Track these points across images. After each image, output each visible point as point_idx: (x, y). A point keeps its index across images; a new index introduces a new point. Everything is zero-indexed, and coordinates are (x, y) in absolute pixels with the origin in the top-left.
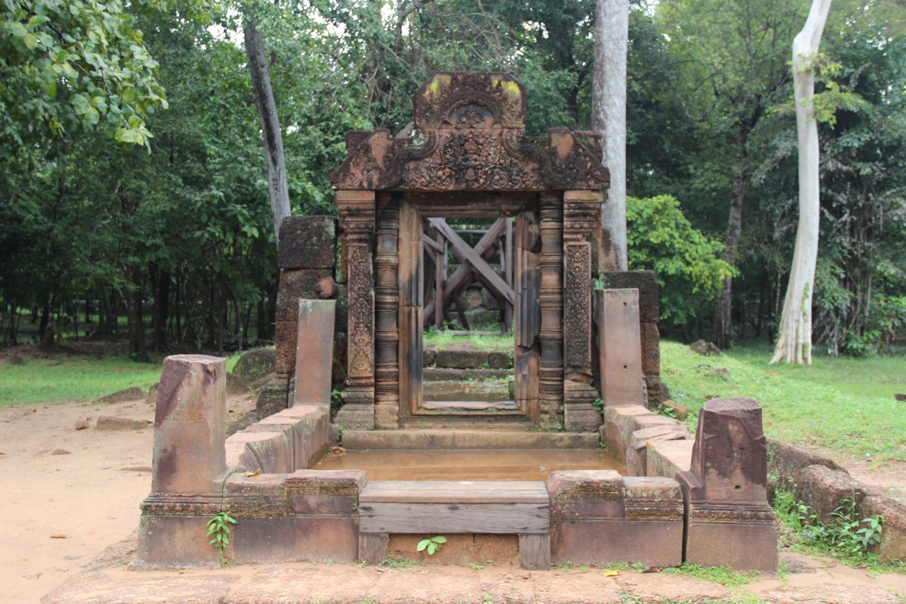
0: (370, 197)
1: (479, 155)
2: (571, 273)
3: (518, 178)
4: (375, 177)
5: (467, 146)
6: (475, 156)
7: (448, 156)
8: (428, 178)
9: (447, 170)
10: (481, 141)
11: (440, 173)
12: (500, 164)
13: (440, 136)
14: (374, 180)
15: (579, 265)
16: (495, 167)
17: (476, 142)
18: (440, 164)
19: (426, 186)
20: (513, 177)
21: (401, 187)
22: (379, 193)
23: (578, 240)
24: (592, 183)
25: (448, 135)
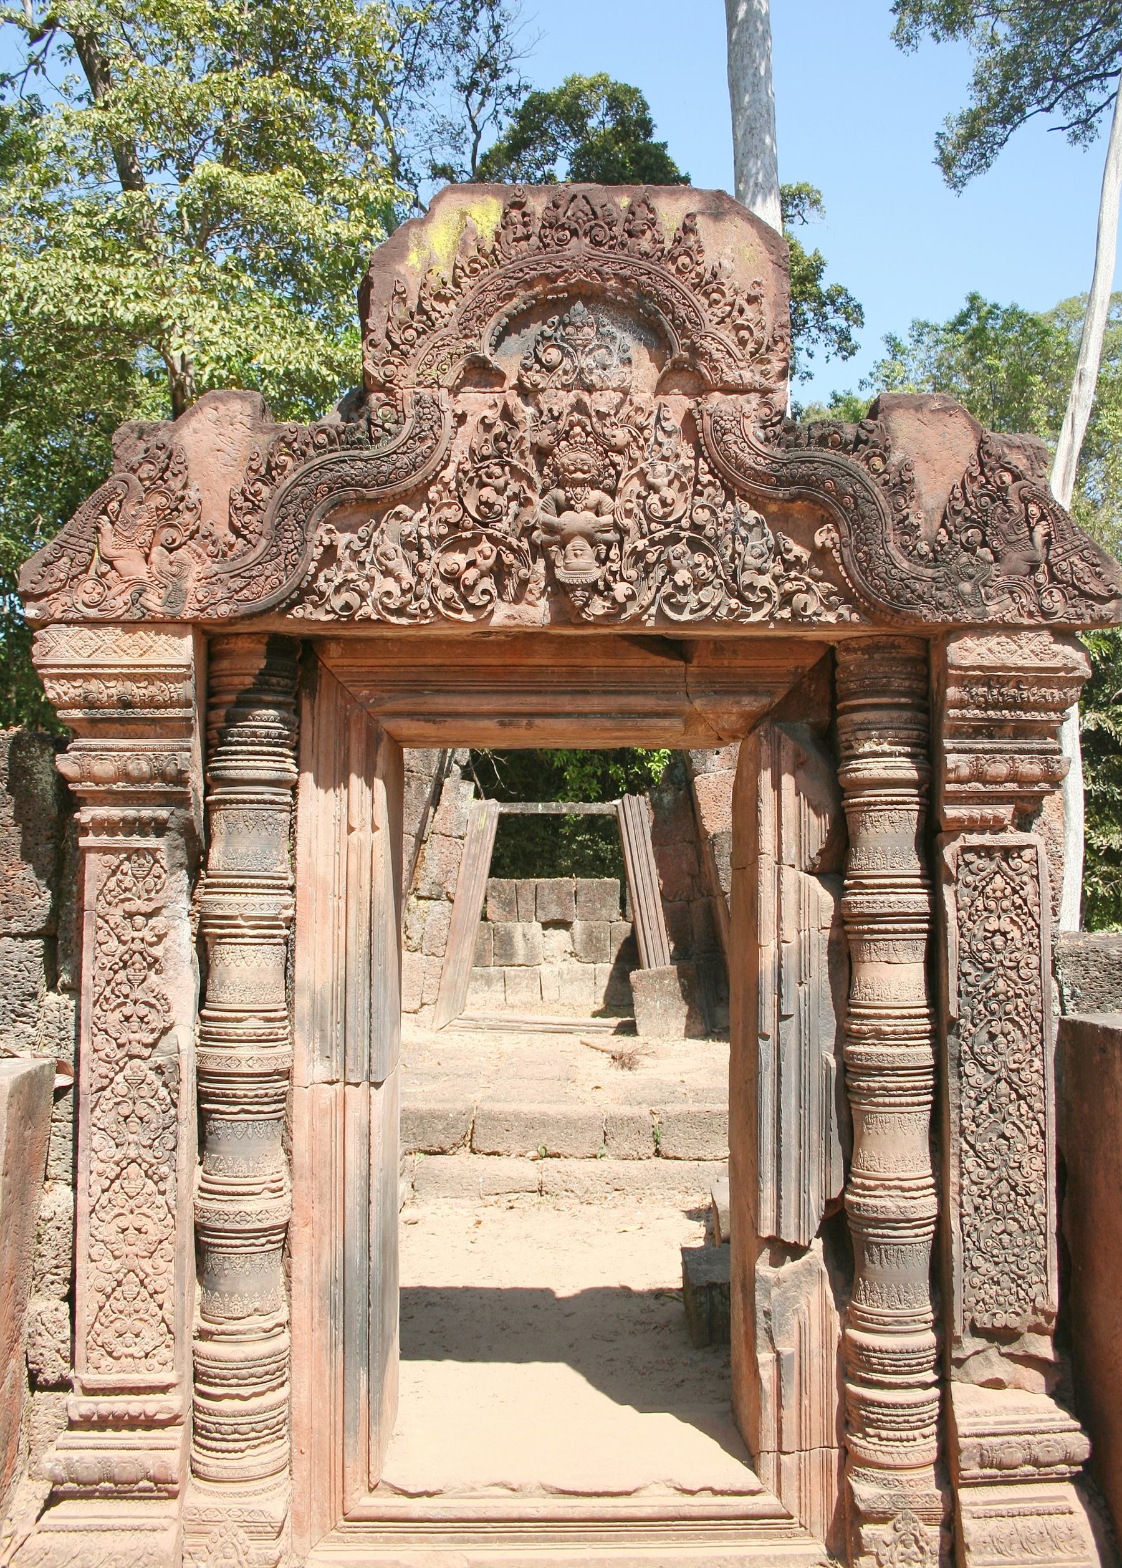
0: (181, 650)
1: (613, 492)
2: (974, 958)
3: (765, 581)
4: (195, 568)
5: (566, 456)
6: (595, 495)
7: (487, 493)
8: (406, 573)
9: (485, 545)
10: (621, 436)
11: (458, 559)
12: (696, 527)
13: (461, 419)
14: (190, 584)
15: (1005, 924)
16: (674, 539)
17: (599, 438)
18: (455, 526)
19: (400, 612)
20: (745, 578)
21: (298, 612)
22: (212, 641)
23: (997, 827)
24: (1055, 601)
25: (492, 415)
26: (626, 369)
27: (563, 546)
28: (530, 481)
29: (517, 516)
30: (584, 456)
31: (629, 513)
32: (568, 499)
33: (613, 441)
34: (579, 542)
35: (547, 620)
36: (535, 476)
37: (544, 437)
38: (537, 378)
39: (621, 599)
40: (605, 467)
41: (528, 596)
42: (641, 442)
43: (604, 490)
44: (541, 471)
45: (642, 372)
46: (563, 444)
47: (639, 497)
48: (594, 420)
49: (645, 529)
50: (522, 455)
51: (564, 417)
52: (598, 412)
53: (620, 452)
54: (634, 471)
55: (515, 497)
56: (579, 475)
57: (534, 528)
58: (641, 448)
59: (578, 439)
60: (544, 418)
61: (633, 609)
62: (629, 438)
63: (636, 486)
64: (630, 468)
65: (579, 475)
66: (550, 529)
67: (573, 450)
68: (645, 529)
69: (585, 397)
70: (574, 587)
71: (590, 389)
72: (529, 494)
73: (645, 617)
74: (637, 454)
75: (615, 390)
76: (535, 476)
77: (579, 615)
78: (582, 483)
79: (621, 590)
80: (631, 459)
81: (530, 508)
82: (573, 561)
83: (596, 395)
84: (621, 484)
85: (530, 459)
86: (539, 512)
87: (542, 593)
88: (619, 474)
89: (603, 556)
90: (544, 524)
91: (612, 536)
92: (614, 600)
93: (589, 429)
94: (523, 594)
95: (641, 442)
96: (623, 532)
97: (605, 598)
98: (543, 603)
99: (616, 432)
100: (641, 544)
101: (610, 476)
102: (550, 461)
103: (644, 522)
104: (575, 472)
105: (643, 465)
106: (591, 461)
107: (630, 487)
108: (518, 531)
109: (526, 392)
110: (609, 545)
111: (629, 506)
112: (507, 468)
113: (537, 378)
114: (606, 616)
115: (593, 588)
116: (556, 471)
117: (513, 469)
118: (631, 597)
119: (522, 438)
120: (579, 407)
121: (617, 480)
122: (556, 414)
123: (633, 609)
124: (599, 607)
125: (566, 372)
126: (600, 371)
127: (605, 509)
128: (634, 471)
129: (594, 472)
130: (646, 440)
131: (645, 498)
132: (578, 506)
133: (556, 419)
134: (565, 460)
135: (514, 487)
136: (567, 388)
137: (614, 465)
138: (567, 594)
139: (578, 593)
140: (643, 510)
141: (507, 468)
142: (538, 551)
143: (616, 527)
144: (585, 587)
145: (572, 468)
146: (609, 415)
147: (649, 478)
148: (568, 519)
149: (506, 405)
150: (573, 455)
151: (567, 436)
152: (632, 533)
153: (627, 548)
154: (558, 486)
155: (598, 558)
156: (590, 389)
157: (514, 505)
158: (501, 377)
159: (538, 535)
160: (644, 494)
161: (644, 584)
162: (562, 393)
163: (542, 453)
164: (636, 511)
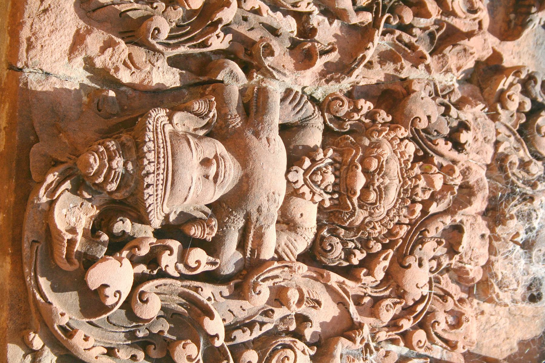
1: (312, 256)
10: (417, 280)
26: (521, 290)
27: (216, 131)
28: (343, 68)
29: (274, 32)
30: (393, 194)
31: (279, 297)
32: (310, 152)
33: (411, 261)
34: (232, 172)
35: (34, 81)
36: (346, 84)
37: (425, 109)
38: (513, 106)
39: (95, 278)
40: (365, 244)
41: (95, 40)
42: (407, 324)
43: (318, 240)
44: (367, 92)
45: (504, 323)
46: (411, 148)
47: (302, 319)
48: (448, 220)
49: (242, 337)
50: (385, 57)
51: (454, 155)
52: (458, 229)
53: (390, 277)
54: (353, 309)
55: (307, 32)
56: (361, 181)
57: (247, 69)
58: (394, 324)
59: (422, 183)
60: (454, 112)
61: (64, 307)
62: (414, 294)
63: (327, 313)
64: (358, 300)
65: (361, 181)
66: (254, 106)
67: (404, 173)
68: (242, 337)
69: (479, 204)
70: (135, 151)
71: (494, 215)
72: (320, 63)
73: (37, 342)
74: (387, 316)
75: (488, 266)
76: (346, 84)
77: (55, 164)
78: (343, 188)
79: (115, 276)
80: (377, 301)
81: (289, 62)
82: (191, 159)
83: (482, 226)
84: (335, 278)
85: (377, 75)
86: (287, 80)
87: (104, 77)
88: (349, 272)
89: (195, 231)
90: (263, 94)
91: (230, 257)
92: (89, 261)
93: (434, 209)
94: (101, 23)
95: (407, 324)
96: (239, 285)
97: (92, 233)
98: (72, 76)
99: (427, 265)
100: (215, 326)
101: (349, 254)
102: (383, 116)
103: (257, 333)
104: (366, 172)
105: (366, 331)
106: (381, 212)
107: (325, 298)
108: (243, 29)
109: (485, 76)
110: (213, 248)
111: (293, 296)
112: (368, 17)
113: (513, 106)
114: (49, 234)
115: (128, 203)
116: (359, 130)
117: (362, 35)
118: (93, 303)
119: (418, 60)
120: (467, 192)
121: (338, 270)
122: (464, 137)
123: (64, 307)
124: (72, 215)
125: (524, 165)
126: (523, 236)
127: (285, 237)
128: (353, 309)
129: (360, 216)
130: (406, 336)
131: (298, 335)
132: (298, 176)
133: (453, 139)
134: (387, 150)
135: (327, 32)
136: (499, 163)
137: (368, 263)
138: (107, 134)
139: (118, 163)
140: (274, 334)
141: (368, 17)
142: (201, 75)
143: (251, 266)
144: (134, 183)
145: (374, 164)
146: (452, 251)
147: (342, 346)
148: (272, 154)
149: (470, 35)
150: (394, 168)
151: (423, 158)
152: (234, 305)
153: (207, 292)
154: (327, 132)
155: (187, 219)
156: (494, 215)
157: (289, 26)
158: (509, 30)
159: (234, 78)
160: (308, 333)
161: (118, 338)
162: (490, 150)
163: (393, 98)
164: (279, 313)
